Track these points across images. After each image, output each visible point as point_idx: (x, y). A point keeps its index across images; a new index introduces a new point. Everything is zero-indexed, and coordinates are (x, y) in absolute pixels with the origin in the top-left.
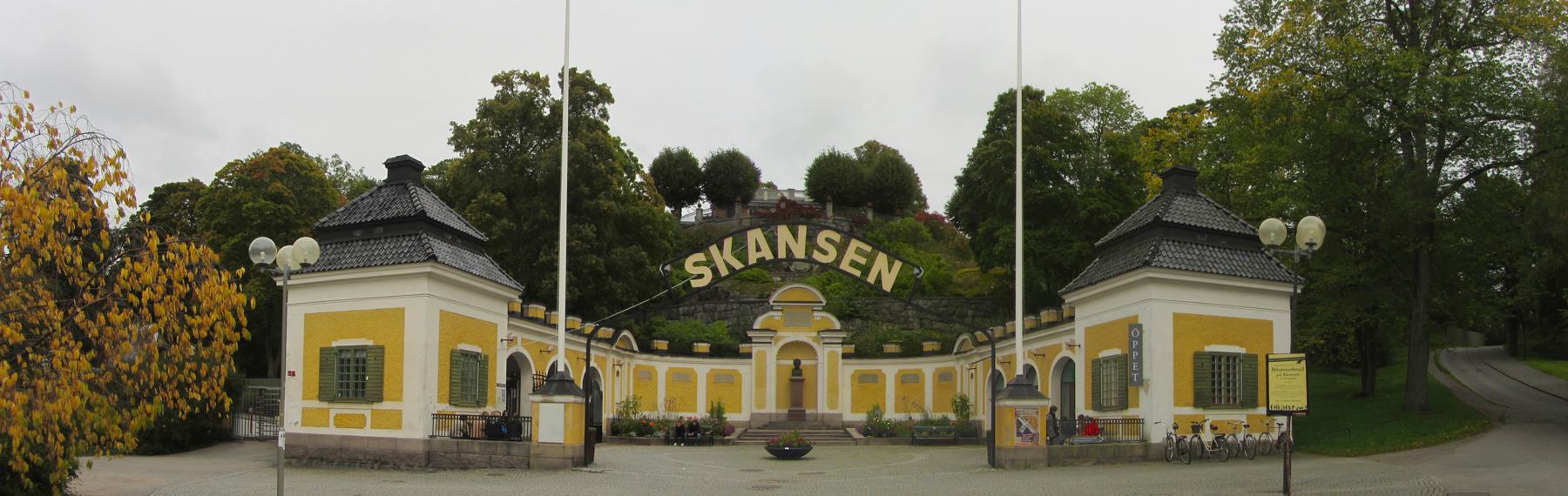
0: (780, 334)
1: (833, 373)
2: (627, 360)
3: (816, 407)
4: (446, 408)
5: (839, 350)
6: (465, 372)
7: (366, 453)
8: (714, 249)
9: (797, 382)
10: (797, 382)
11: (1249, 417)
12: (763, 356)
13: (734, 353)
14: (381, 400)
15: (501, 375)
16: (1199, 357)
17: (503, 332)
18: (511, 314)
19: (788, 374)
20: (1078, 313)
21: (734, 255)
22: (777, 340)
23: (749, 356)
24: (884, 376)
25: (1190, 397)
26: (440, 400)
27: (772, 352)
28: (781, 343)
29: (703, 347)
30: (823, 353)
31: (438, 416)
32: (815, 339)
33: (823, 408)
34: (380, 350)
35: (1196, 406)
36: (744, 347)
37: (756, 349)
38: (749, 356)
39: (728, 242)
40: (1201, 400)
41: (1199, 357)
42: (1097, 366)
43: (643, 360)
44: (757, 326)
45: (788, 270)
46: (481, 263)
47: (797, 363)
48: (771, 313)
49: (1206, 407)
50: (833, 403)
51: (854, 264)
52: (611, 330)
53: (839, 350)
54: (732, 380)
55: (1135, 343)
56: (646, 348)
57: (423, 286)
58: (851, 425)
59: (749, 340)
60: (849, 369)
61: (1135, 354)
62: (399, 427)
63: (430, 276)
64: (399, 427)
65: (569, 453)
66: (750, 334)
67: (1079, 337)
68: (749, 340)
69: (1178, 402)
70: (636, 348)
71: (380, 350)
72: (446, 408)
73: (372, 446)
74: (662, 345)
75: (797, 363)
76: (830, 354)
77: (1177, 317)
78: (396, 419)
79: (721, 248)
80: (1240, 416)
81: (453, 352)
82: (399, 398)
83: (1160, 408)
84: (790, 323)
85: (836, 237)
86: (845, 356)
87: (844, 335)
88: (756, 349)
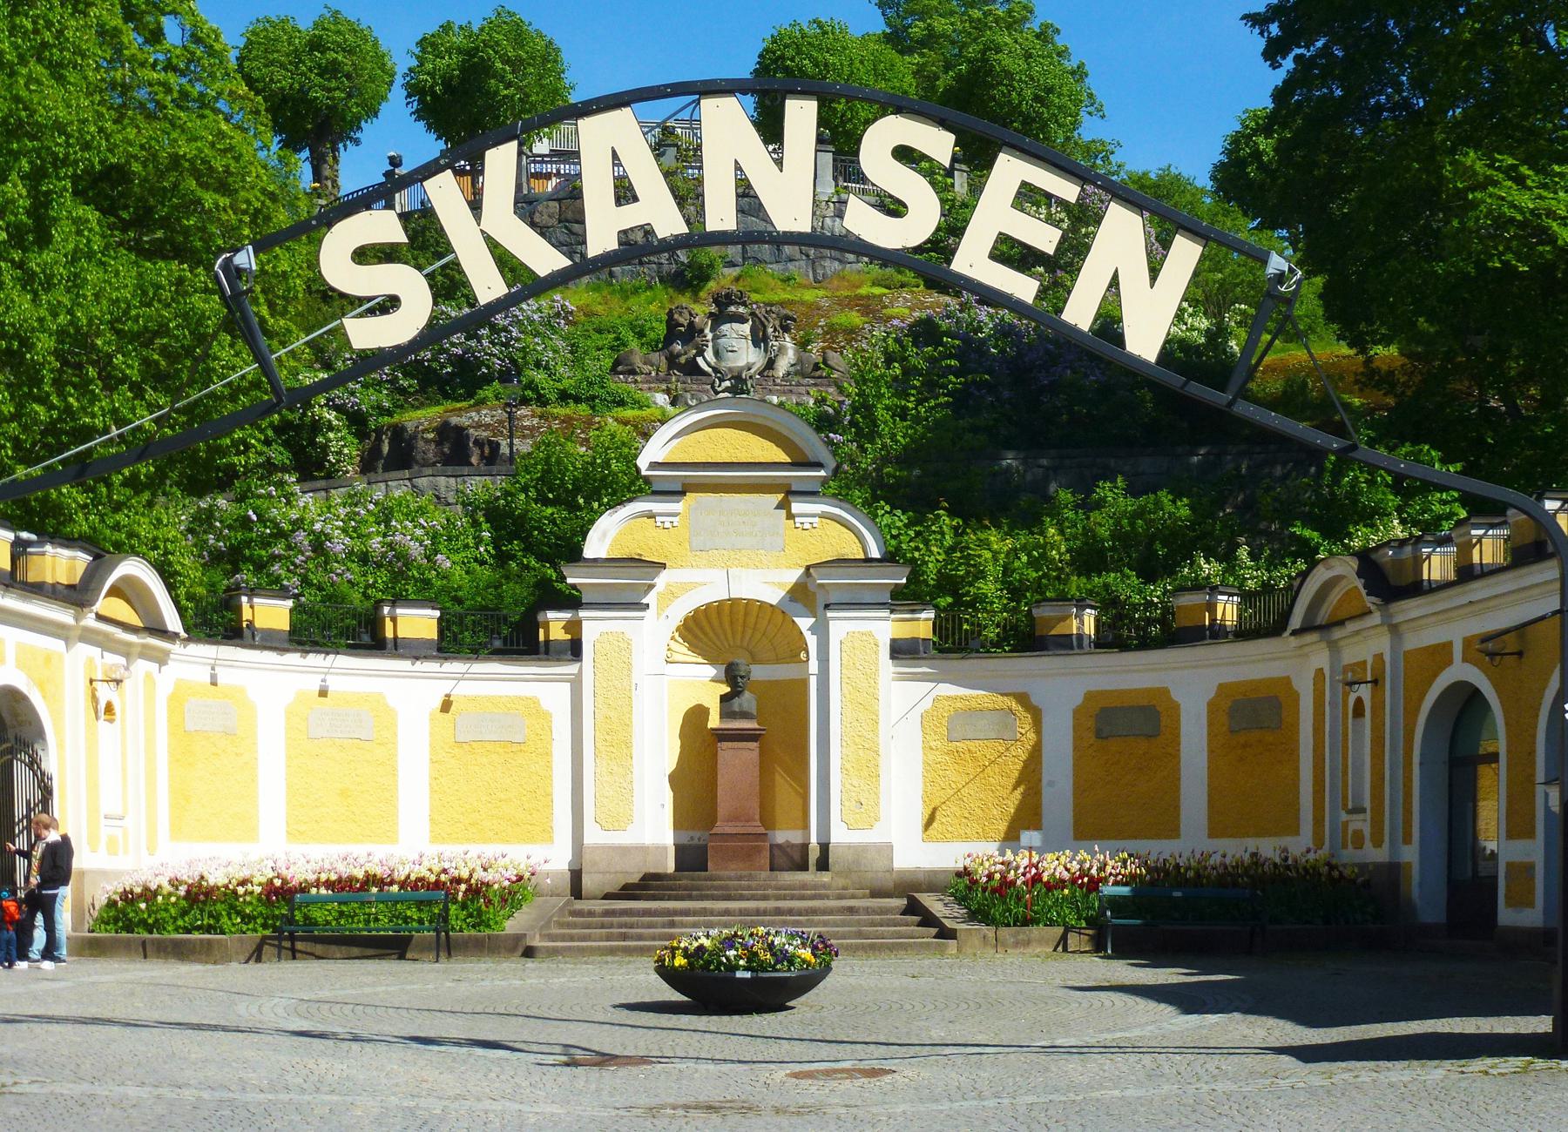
1: (867, 706)
2: (142, 666)
10: (755, 732)
23: (574, 649)
29: (417, 622)
36: (555, 623)
43: (195, 661)
44: (594, 547)
50: (866, 809)
52: (82, 559)
56: (217, 622)
58: (932, 882)
59: (572, 601)
70: (173, 622)
74: (271, 613)
85: (939, 144)
86: (902, 650)
88: (596, 628)
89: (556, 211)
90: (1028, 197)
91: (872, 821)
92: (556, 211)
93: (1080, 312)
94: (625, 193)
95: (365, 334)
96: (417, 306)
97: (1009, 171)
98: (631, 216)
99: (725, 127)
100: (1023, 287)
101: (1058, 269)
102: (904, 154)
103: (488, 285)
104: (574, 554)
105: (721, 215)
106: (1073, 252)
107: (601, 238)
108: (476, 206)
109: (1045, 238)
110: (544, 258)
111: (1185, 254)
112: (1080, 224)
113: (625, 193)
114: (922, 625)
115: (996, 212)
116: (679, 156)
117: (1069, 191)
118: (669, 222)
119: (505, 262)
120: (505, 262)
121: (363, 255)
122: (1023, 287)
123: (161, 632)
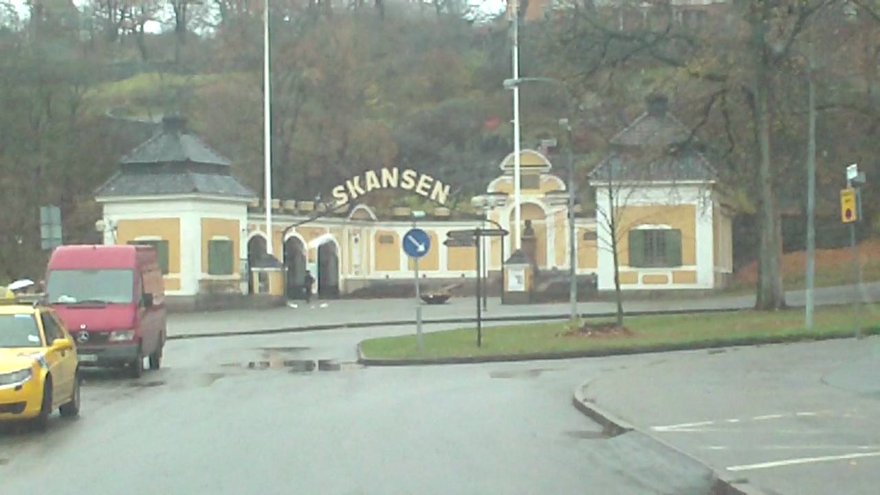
3: (545, 263)
4: (207, 276)
6: (218, 254)
15: (243, 253)
17: (244, 224)
26: (203, 271)
31: (201, 281)
32: (543, 200)
34: (165, 243)
44: (490, 190)
48: (503, 177)
49: (638, 266)
57: (189, 205)
62: (178, 288)
63: (194, 200)
70: (373, 216)
71: (165, 243)
72: (207, 276)
78: (176, 284)
82: (178, 271)
89: (363, 184)
90: (426, 181)
92: (363, 184)
93: (433, 197)
94: (372, 182)
96: (346, 199)
97: (424, 177)
98: (373, 185)
99: (385, 172)
100: (425, 194)
101: (430, 191)
102: (409, 175)
105: (385, 185)
106: (433, 188)
107: (369, 189)
108: (353, 184)
109: (428, 187)
110: (362, 192)
111: (447, 188)
112: (433, 185)
113: (372, 182)
115: (421, 183)
116: (379, 177)
118: (378, 186)
119: (356, 191)
120: (356, 191)
122: (425, 194)
123: (371, 220)
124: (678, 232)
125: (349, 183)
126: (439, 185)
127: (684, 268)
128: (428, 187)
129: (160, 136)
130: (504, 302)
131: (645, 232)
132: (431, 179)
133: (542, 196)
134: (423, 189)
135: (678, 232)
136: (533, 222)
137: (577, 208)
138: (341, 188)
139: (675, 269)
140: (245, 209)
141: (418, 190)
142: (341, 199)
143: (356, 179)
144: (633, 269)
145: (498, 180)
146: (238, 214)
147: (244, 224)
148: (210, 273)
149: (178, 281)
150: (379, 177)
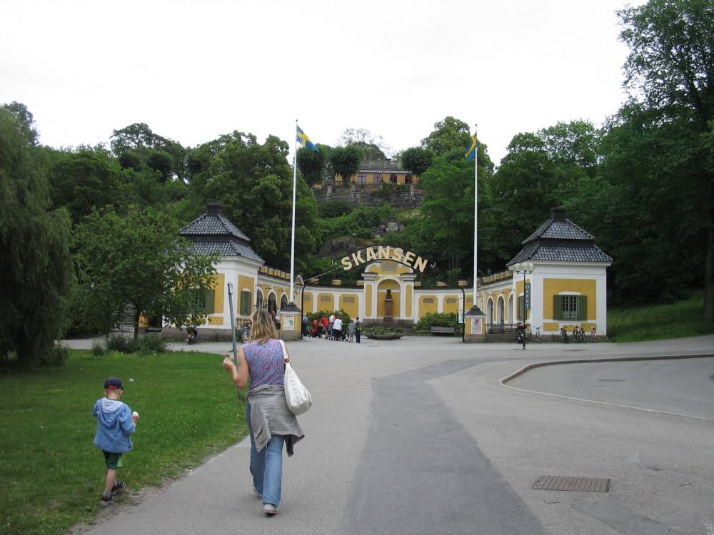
0: (379, 275)
4: (240, 316)
5: (412, 284)
7: (205, 335)
8: (353, 255)
9: (389, 302)
10: (389, 302)
11: (582, 324)
12: (370, 287)
13: (355, 286)
14: (213, 312)
15: (255, 302)
16: (556, 298)
18: (260, 273)
19: (384, 298)
20: (515, 274)
21: (361, 257)
22: (378, 278)
23: (362, 287)
24: (437, 299)
25: (552, 315)
27: (375, 285)
28: (381, 280)
29: (338, 282)
30: (403, 286)
31: (238, 319)
33: (403, 316)
35: (555, 318)
36: (359, 282)
37: (366, 284)
38: (362, 287)
39: (359, 252)
40: (558, 316)
41: (556, 298)
42: (519, 299)
45: (385, 230)
46: (247, 252)
47: (389, 292)
49: (559, 319)
50: (409, 312)
51: (408, 261)
53: (412, 284)
54: (351, 300)
55: (527, 291)
57: (233, 265)
59: (363, 279)
60: (418, 296)
61: (527, 296)
62: (222, 324)
63: (236, 261)
64: (222, 324)
65: (296, 334)
66: (363, 275)
67: (514, 287)
68: (363, 279)
69: (545, 317)
72: (240, 316)
73: (209, 333)
75: (389, 292)
76: (408, 287)
77: (545, 280)
78: (221, 321)
79: (356, 255)
80: (579, 324)
81: (242, 292)
83: (538, 320)
84: (384, 269)
87: (415, 276)
88: (366, 284)
90: (411, 256)
91: (410, 316)
92: (364, 256)
94: (371, 255)
95: (345, 269)
97: (409, 253)
101: (413, 264)
103: (357, 264)
104: (364, 272)
107: (368, 260)
108: (356, 255)
109: (412, 260)
110: (363, 261)
111: (426, 262)
112: (415, 259)
113: (371, 255)
114: (419, 284)
116: (376, 251)
117: (414, 255)
119: (358, 261)
120: (358, 261)
121: (346, 261)
122: (410, 265)
124: (586, 297)
125: (353, 255)
126: (419, 259)
127: (589, 321)
128: (412, 260)
129: (205, 217)
130: (464, 341)
131: (563, 297)
132: (414, 255)
133: (399, 276)
134: (408, 261)
135: (586, 297)
136: (392, 291)
137: (419, 284)
138: (348, 258)
139: (583, 322)
140: (256, 271)
141: (405, 262)
142: (348, 266)
143: (359, 252)
144: (556, 321)
145: (371, 265)
146: (252, 273)
147: (256, 282)
148: (241, 314)
149: (222, 318)
150: (376, 251)
